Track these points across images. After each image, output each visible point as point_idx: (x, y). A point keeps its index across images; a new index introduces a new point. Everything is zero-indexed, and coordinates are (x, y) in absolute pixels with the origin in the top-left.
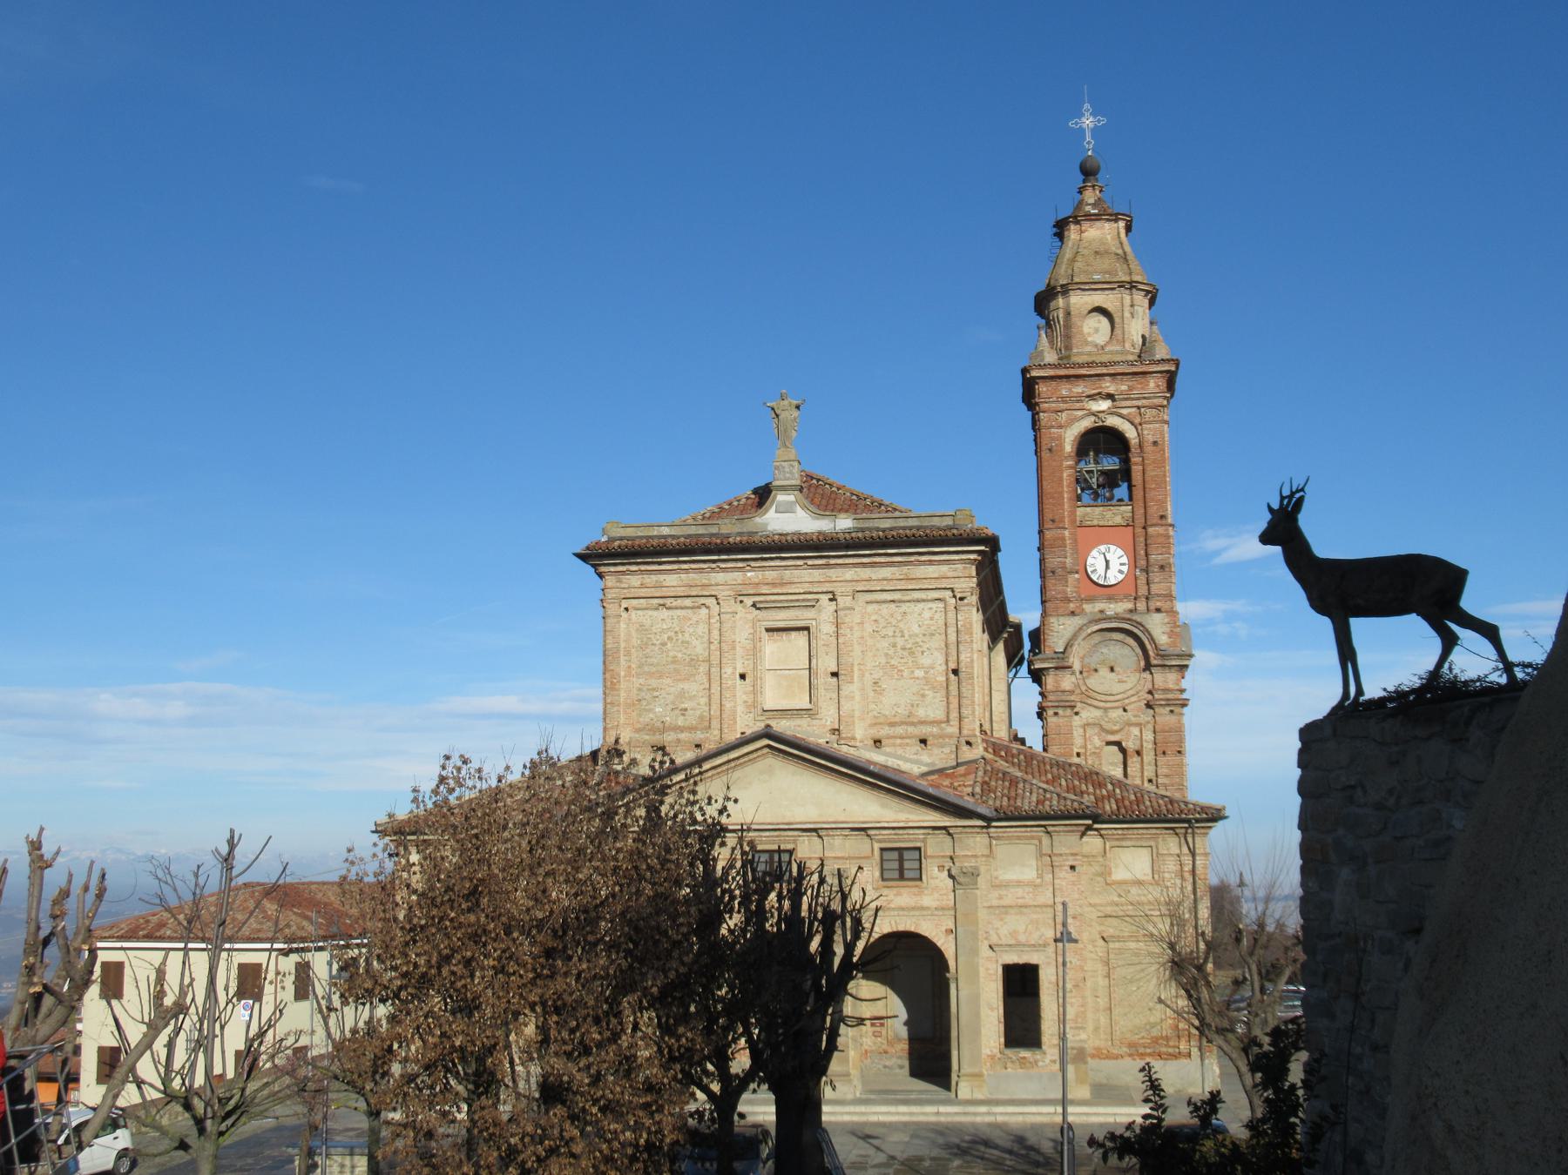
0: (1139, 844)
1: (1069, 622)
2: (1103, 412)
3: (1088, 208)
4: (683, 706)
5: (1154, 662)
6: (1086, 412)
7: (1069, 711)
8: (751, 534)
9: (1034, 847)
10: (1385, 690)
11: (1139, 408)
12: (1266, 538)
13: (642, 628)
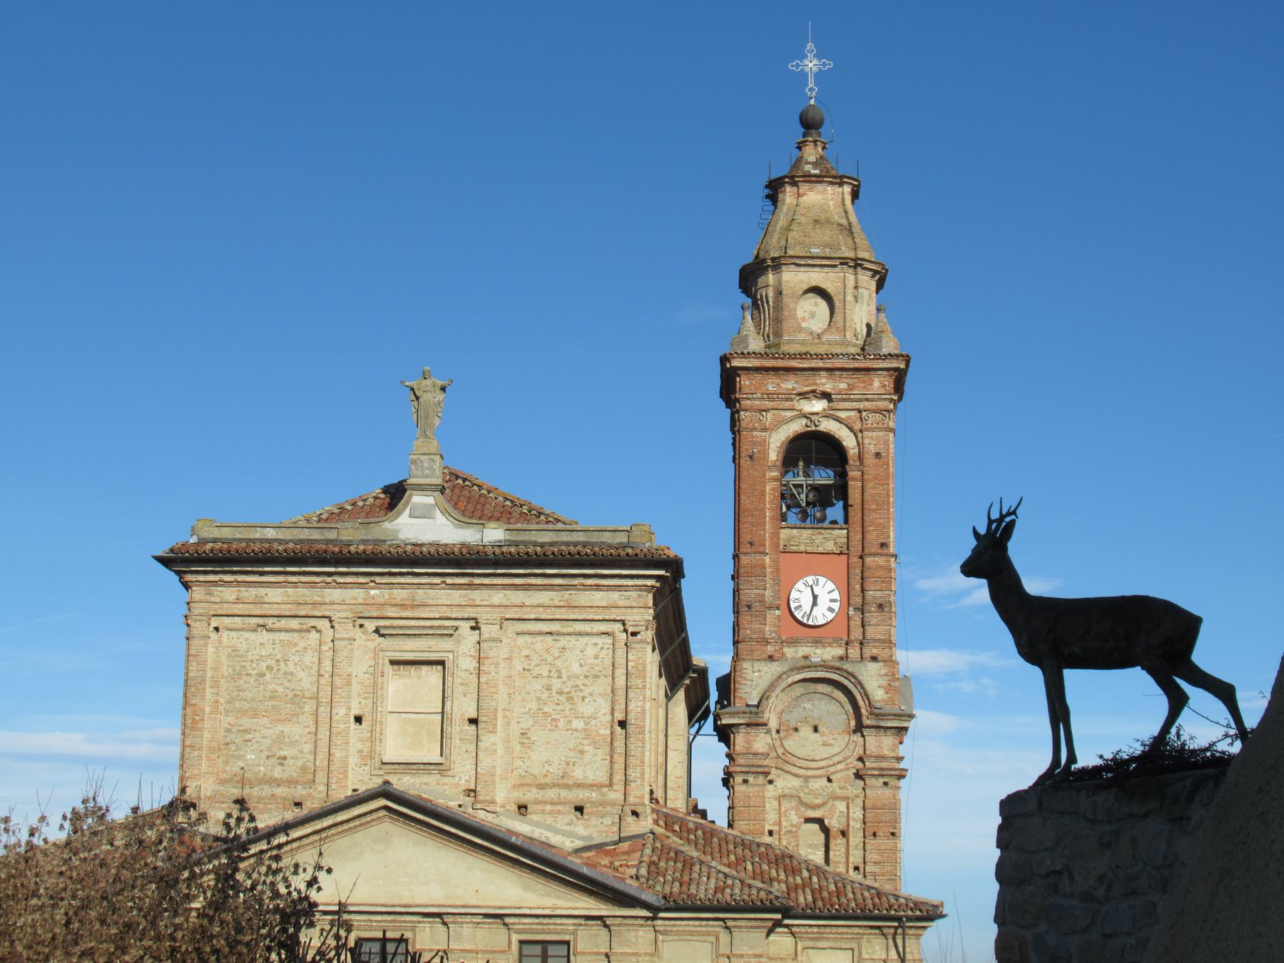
0: (838, 945)
1: (766, 669)
2: (817, 414)
3: (808, 168)
4: (282, 753)
5: (867, 722)
6: (796, 413)
7: (761, 779)
8: (377, 542)
9: (709, 945)
10: (1101, 757)
11: (860, 411)
12: (970, 569)
13: (234, 653)
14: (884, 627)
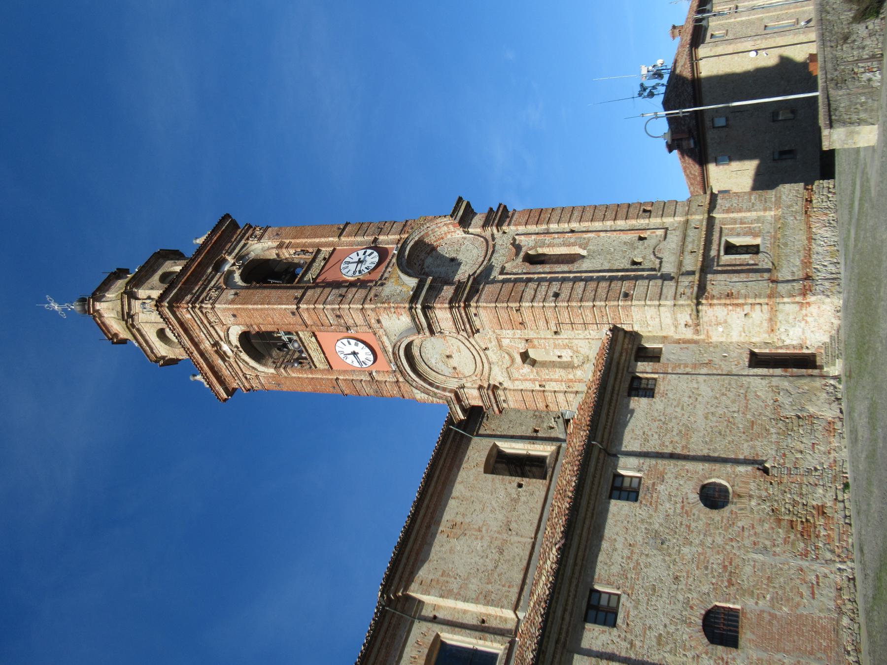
7: (500, 392)
11: (213, 327)
14: (352, 314)
